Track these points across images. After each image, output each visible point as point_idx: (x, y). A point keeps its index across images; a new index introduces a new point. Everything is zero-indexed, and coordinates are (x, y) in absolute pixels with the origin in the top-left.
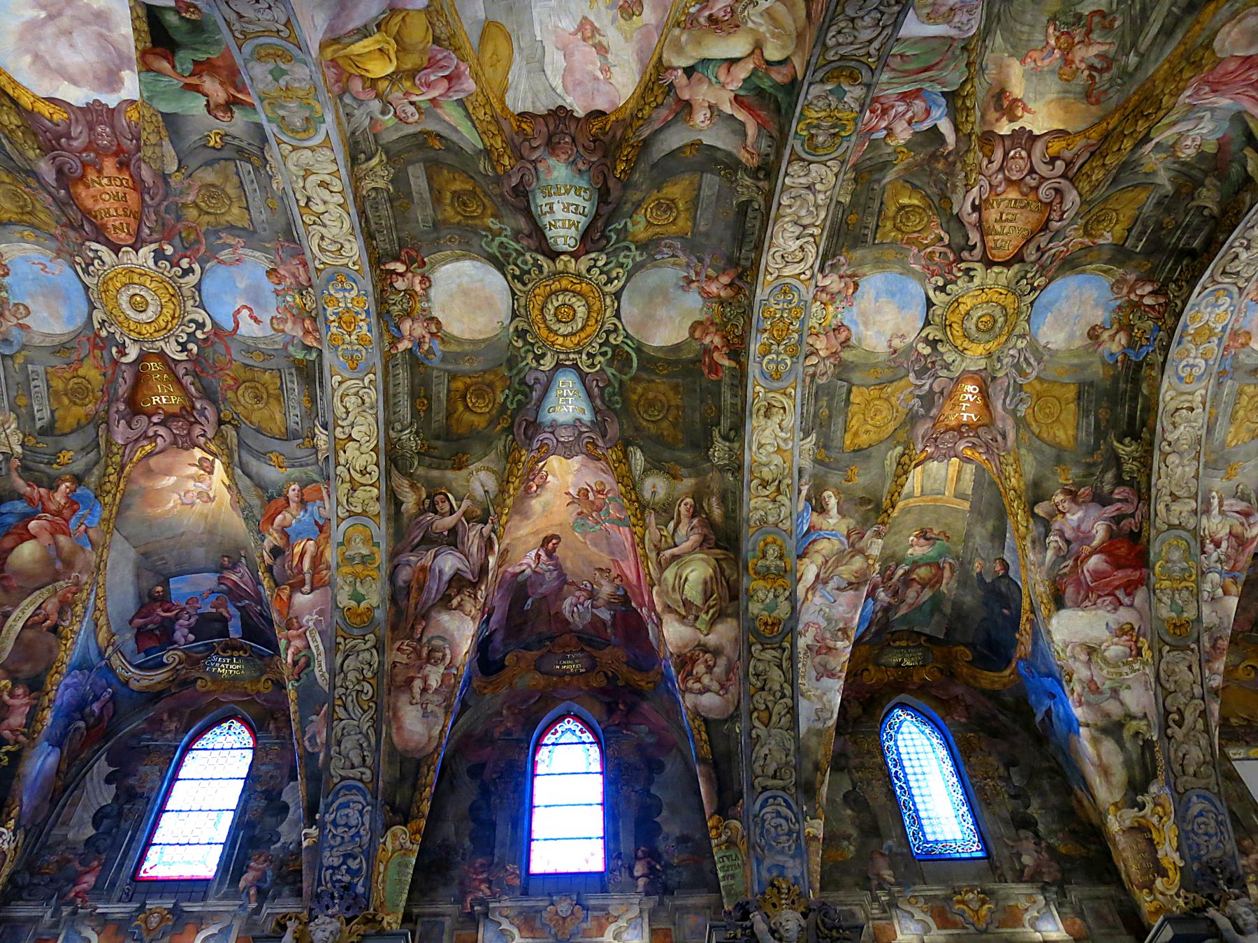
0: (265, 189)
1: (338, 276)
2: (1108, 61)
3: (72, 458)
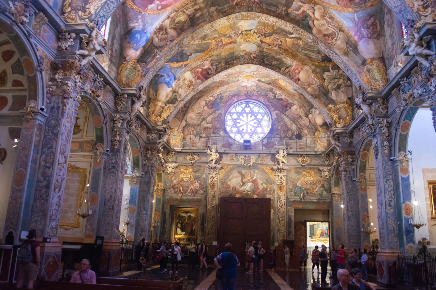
2: (299, 46)
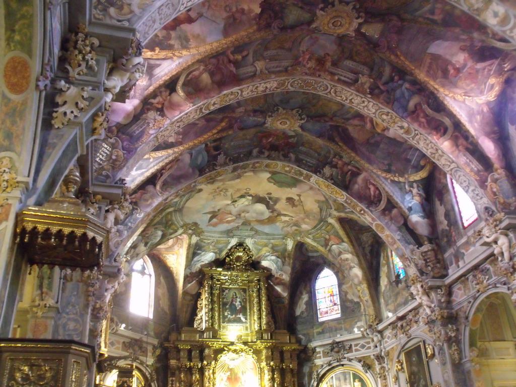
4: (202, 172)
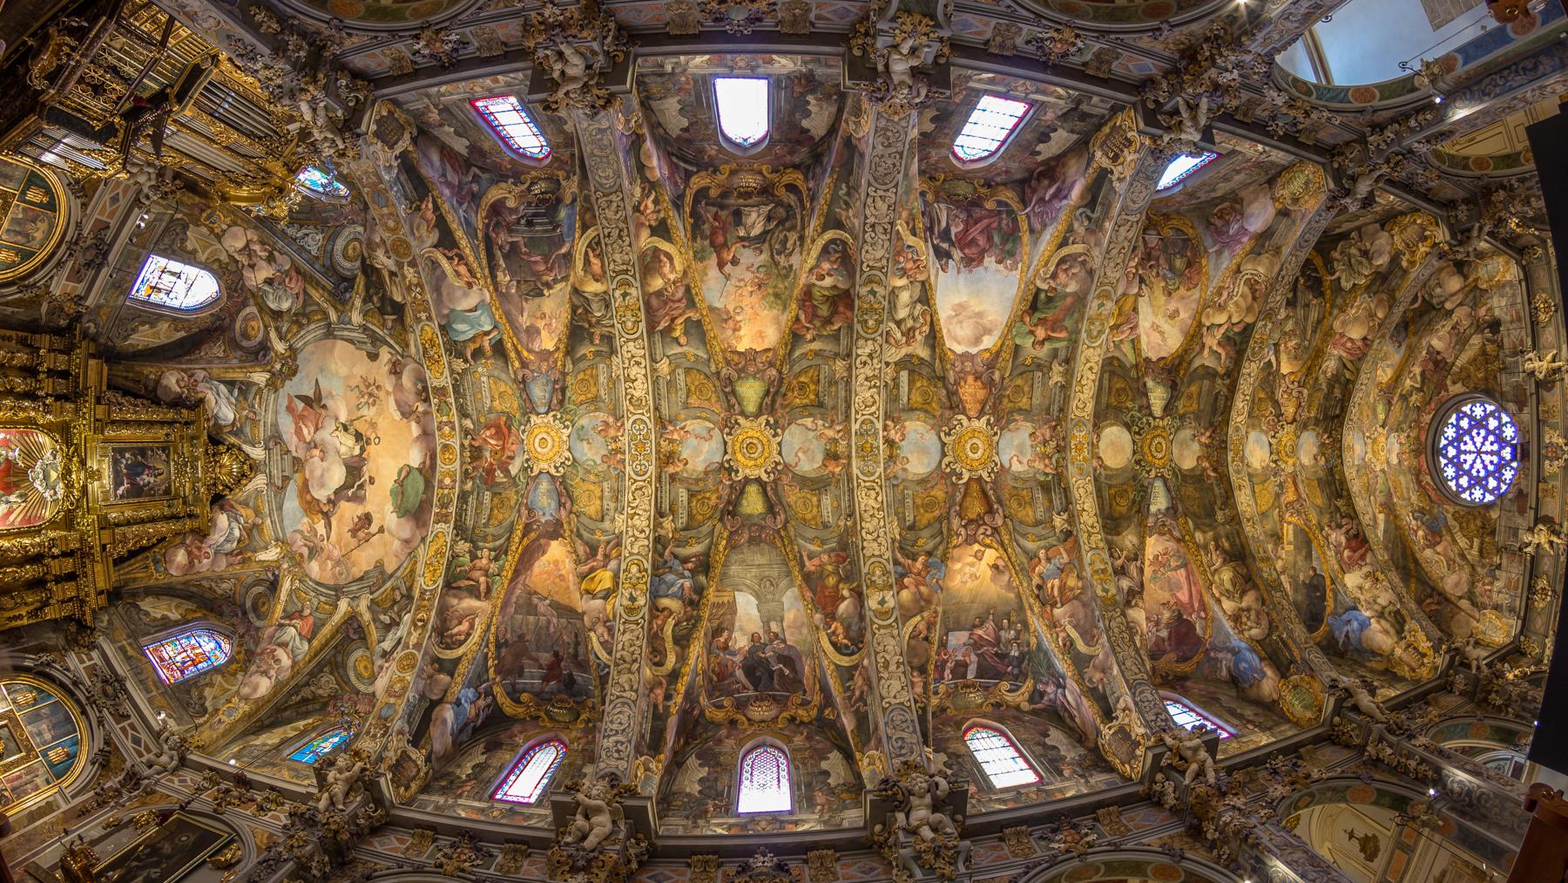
0: (1044, 384)
1: (1080, 423)
3: (925, 541)
4: (444, 329)
